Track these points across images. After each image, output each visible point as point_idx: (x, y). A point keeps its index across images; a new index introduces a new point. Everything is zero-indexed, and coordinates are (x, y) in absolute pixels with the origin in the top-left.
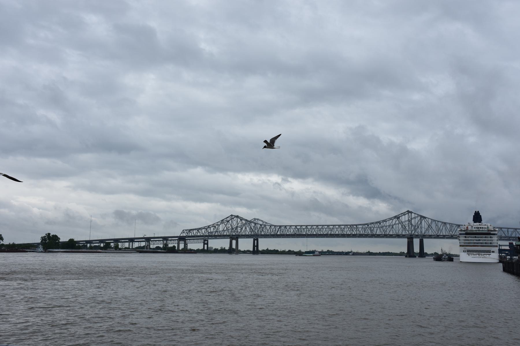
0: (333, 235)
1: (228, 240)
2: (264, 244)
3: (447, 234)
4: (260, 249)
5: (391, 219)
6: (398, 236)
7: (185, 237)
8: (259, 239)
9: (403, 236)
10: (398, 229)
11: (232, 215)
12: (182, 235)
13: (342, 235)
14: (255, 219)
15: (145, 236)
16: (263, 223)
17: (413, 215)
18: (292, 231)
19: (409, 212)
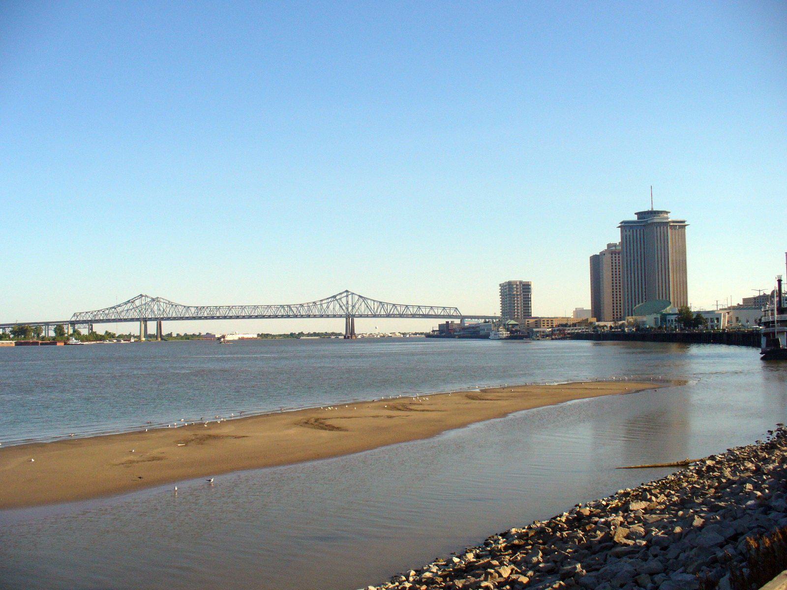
0: (98, 320)
1: (138, 323)
2: (168, 328)
3: (304, 314)
4: (164, 332)
5: (328, 299)
6: (334, 316)
7: (76, 321)
8: (163, 322)
9: (341, 316)
10: (334, 308)
11: (141, 295)
12: (73, 319)
13: (107, 320)
14: (158, 298)
15: (18, 322)
16: (169, 302)
17: (349, 293)
18: (192, 312)
19: (347, 291)
